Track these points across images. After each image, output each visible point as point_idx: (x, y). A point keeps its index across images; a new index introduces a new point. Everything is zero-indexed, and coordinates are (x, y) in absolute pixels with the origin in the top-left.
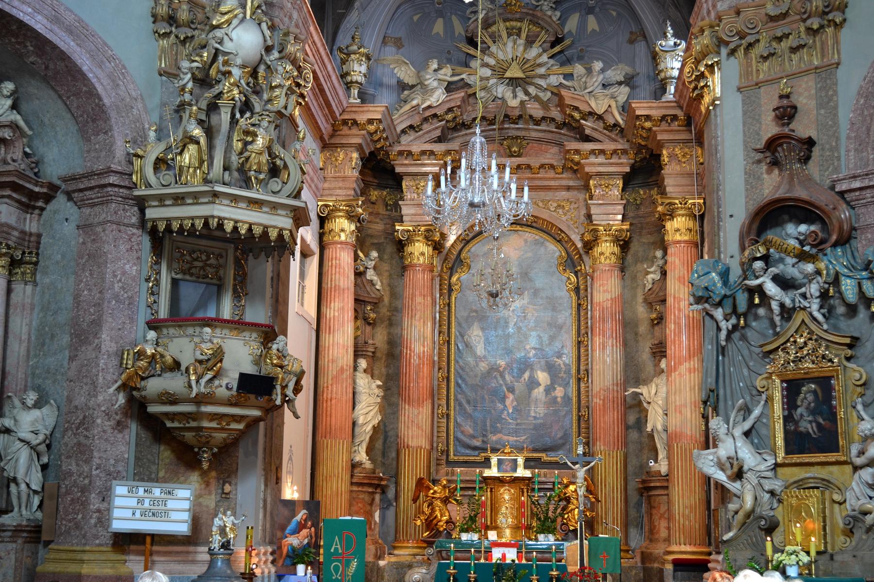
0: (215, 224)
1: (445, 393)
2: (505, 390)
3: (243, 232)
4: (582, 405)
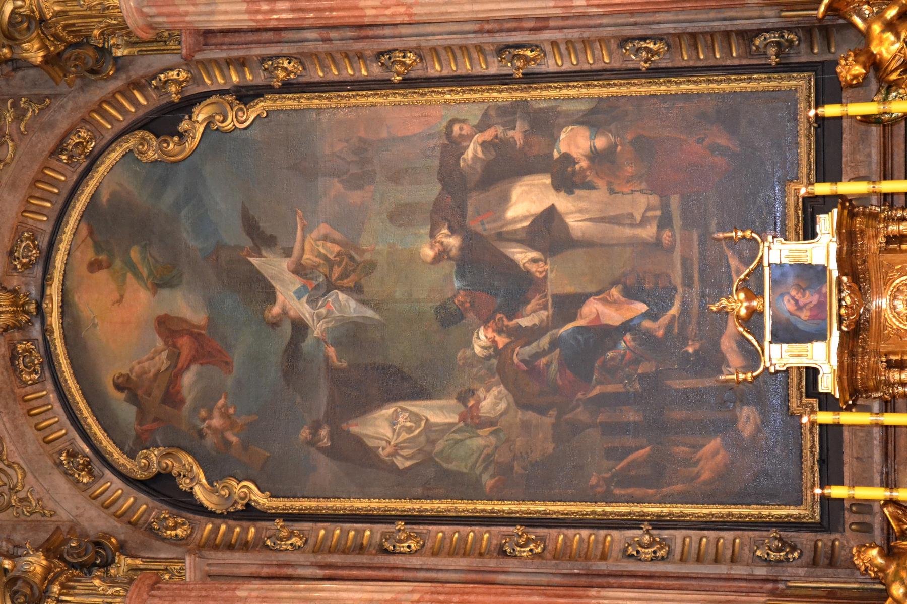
1: (585, 532)
2: (570, 326)
4: (617, 65)
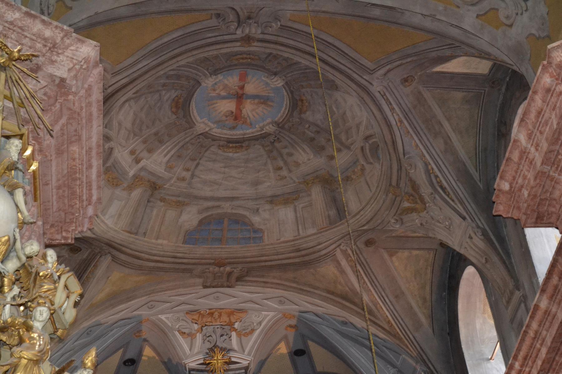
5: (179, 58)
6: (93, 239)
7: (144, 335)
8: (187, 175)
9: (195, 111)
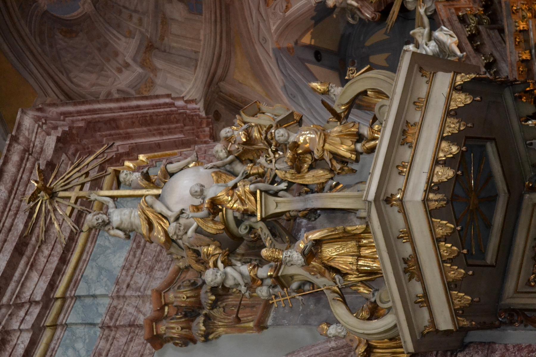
0: (439, 196)
3: (455, 149)
5: (23, 33)
6: (205, 101)
7: (291, 44)
8: (136, 16)
9: (73, 14)
